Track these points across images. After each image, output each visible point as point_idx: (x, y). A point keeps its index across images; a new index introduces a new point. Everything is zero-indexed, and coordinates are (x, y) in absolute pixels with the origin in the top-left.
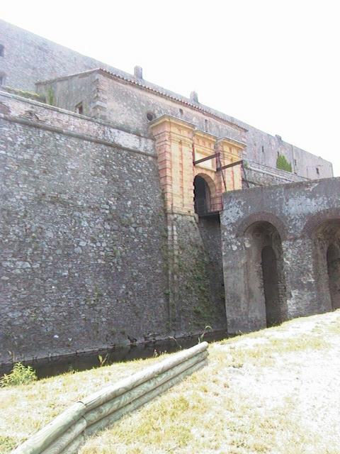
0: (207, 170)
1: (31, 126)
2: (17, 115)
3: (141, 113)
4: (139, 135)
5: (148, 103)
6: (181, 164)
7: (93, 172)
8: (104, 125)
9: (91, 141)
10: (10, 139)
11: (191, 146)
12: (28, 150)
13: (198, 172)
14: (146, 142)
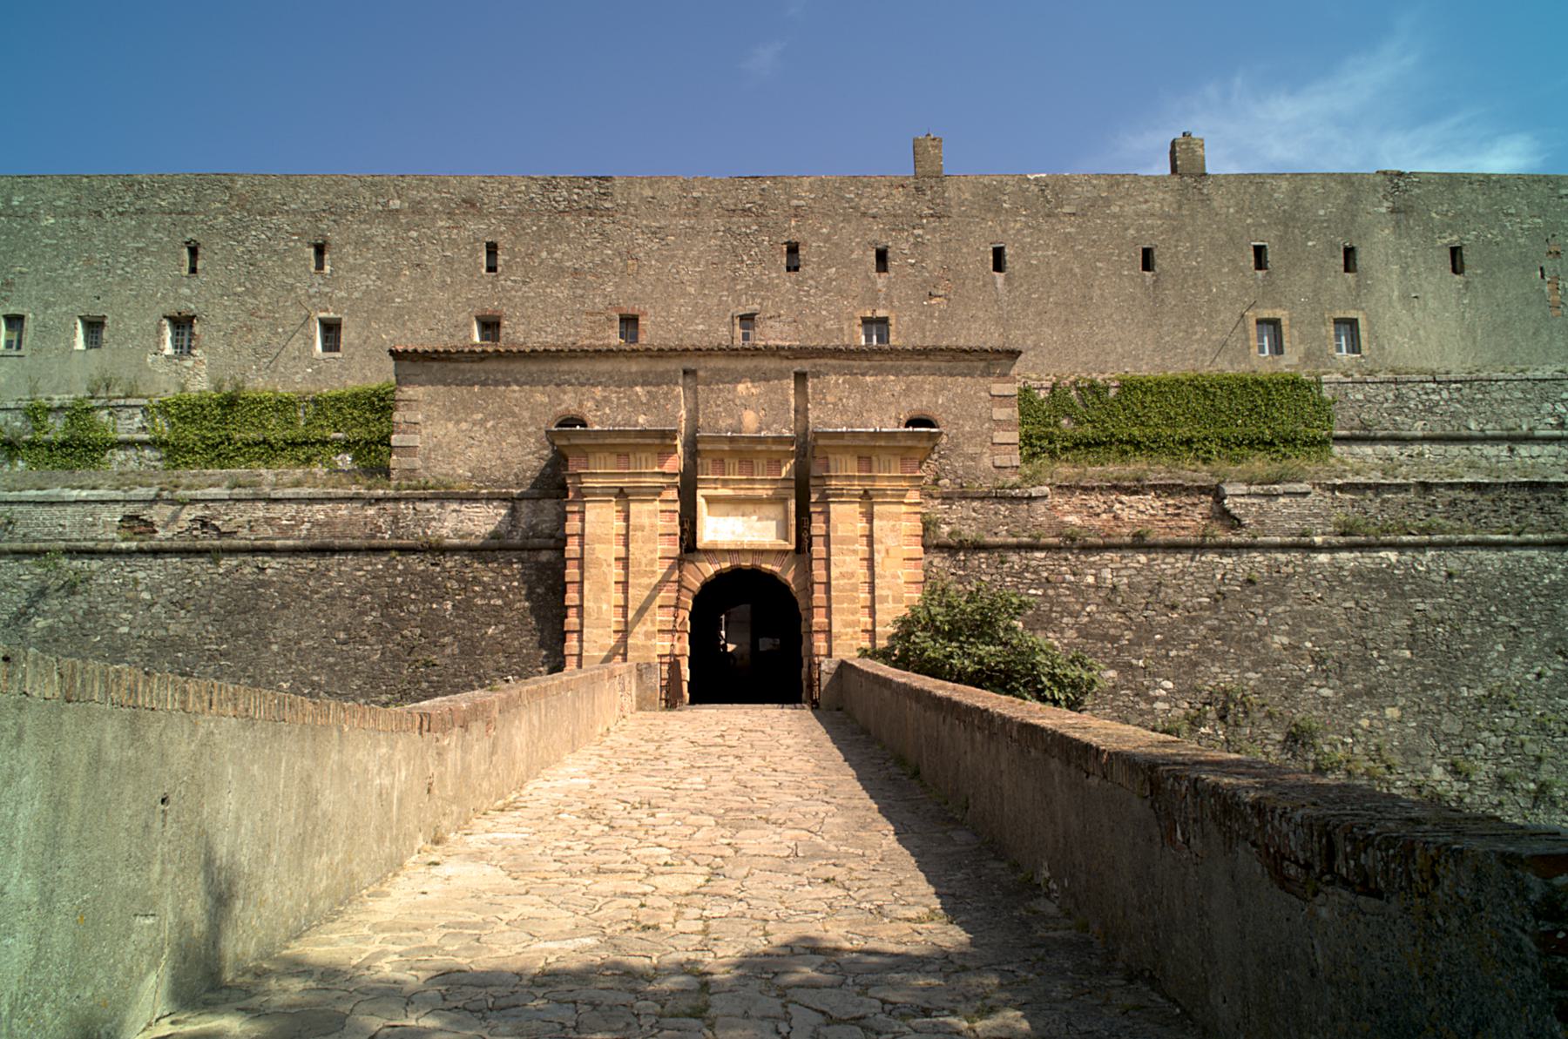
1: (200, 552)
3: (532, 429)
6: (625, 561)
7: (342, 635)
8: (396, 500)
9: (356, 551)
10: (146, 596)
14: (534, 513)
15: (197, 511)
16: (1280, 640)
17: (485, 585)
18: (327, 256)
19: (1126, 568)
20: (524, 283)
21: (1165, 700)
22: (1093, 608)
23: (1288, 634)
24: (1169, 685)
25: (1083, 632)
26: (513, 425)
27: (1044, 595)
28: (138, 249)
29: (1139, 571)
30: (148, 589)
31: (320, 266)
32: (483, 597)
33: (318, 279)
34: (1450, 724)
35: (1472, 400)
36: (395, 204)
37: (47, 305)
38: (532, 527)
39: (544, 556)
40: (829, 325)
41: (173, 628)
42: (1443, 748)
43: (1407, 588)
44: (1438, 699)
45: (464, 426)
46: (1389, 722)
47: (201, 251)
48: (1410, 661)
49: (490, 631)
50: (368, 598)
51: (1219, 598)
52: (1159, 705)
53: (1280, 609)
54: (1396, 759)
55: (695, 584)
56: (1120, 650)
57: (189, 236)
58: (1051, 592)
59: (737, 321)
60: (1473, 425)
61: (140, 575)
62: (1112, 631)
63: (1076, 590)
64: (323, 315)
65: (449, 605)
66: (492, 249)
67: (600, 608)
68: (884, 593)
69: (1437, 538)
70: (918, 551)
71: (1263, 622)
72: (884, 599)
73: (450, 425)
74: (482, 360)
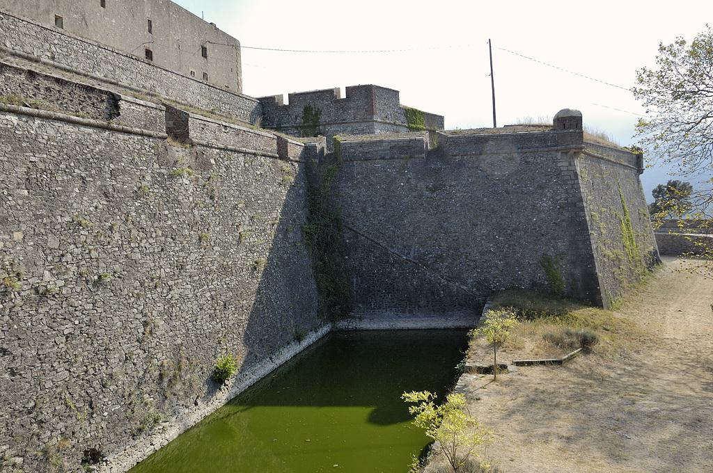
34: (53, 242)
35: (9, 28)
43: (24, 145)
44: (45, 224)
46: (16, 243)
48: (28, 198)
54: (23, 270)
60: (8, 44)
69: (42, 112)
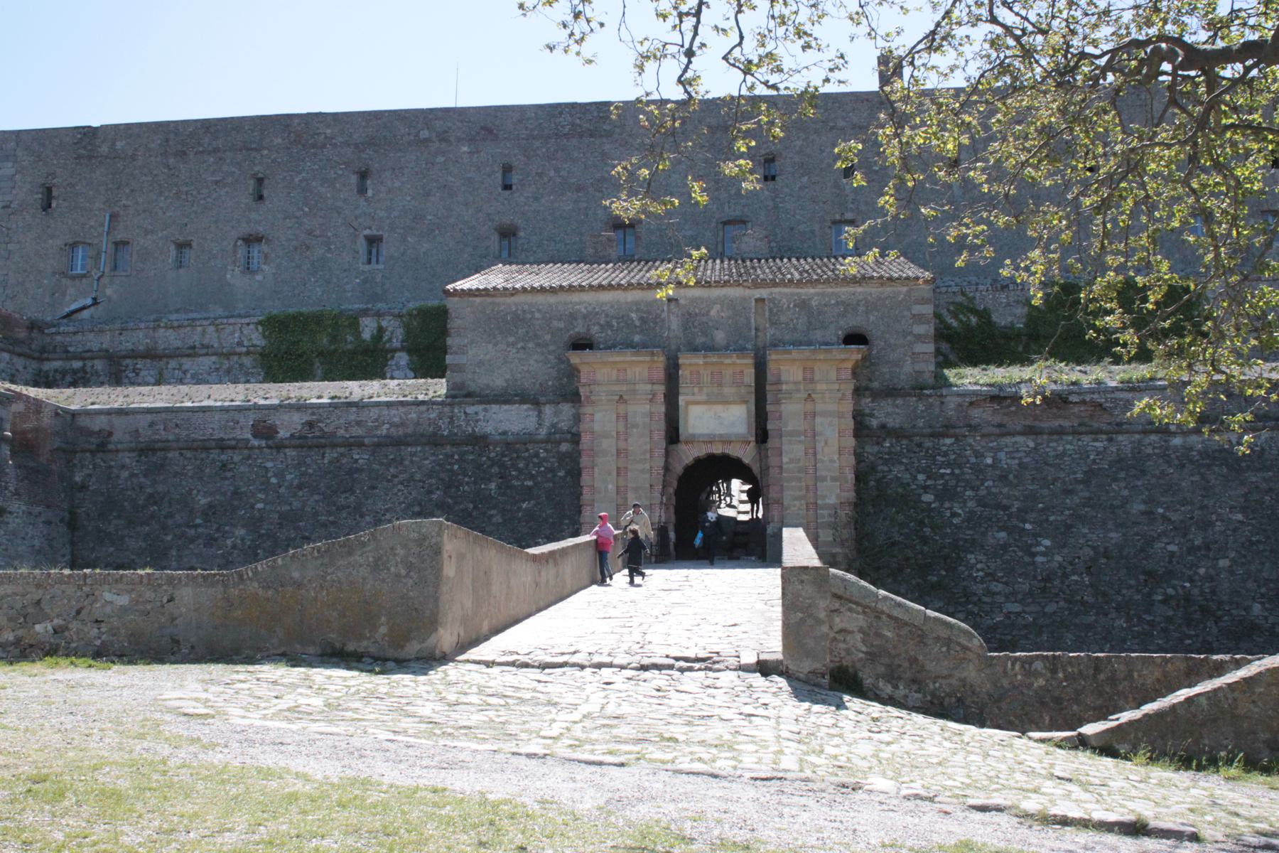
0: (727, 441)
2: (288, 435)
4: (536, 403)
5: (573, 316)
10: (274, 480)
11: (661, 398)
12: (300, 493)
13: (688, 454)
14: (556, 414)
15: (306, 418)
16: (1138, 507)
17: (520, 471)
18: (369, 182)
19: (1018, 451)
20: (536, 199)
21: (1044, 554)
22: (991, 483)
23: (1144, 502)
24: (1047, 542)
25: (981, 502)
26: (538, 345)
27: (952, 474)
28: (217, 182)
29: (1028, 454)
30: (275, 475)
31: (362, 190)
32: (518, 479)
33: (362, 202)
36: (425, 134)
37: (147, 232)
38: (554, 425)
39: (565, 447)
40: (801, 228)
41: (296, 504)
42: (1263, 590)
45: (503, 346)
47: (266, 182)
48: (1241, 522)
49: (524, 506)
50: (434, 481)
51: (1090, 473)
52: (1039, 559)
53: (1139, 483)
55: (679, 469)
56: (1010, 516)
57: (256, 169)
58: (957, 471)
59: (720, 226)
61: (269, 465)
62: (1005, 502)
63: (979, 470)
64: (367, 232)
65: (493, 486)
66: (507, 170)
67: (606, 489)
68: (824, 473)
70: (851, 442)
71: (1125, 493)
72: (823, 479)
73: (490, 346)
74: (512, 295)
